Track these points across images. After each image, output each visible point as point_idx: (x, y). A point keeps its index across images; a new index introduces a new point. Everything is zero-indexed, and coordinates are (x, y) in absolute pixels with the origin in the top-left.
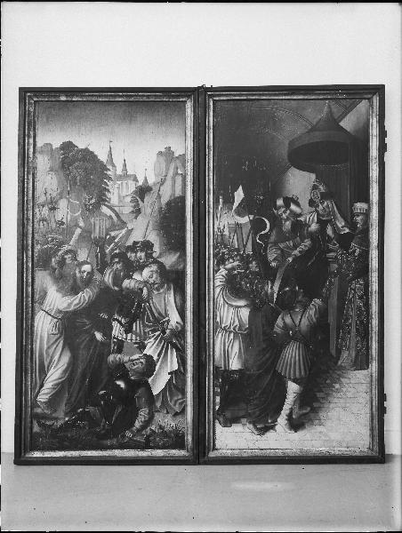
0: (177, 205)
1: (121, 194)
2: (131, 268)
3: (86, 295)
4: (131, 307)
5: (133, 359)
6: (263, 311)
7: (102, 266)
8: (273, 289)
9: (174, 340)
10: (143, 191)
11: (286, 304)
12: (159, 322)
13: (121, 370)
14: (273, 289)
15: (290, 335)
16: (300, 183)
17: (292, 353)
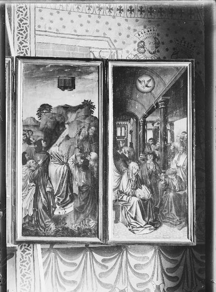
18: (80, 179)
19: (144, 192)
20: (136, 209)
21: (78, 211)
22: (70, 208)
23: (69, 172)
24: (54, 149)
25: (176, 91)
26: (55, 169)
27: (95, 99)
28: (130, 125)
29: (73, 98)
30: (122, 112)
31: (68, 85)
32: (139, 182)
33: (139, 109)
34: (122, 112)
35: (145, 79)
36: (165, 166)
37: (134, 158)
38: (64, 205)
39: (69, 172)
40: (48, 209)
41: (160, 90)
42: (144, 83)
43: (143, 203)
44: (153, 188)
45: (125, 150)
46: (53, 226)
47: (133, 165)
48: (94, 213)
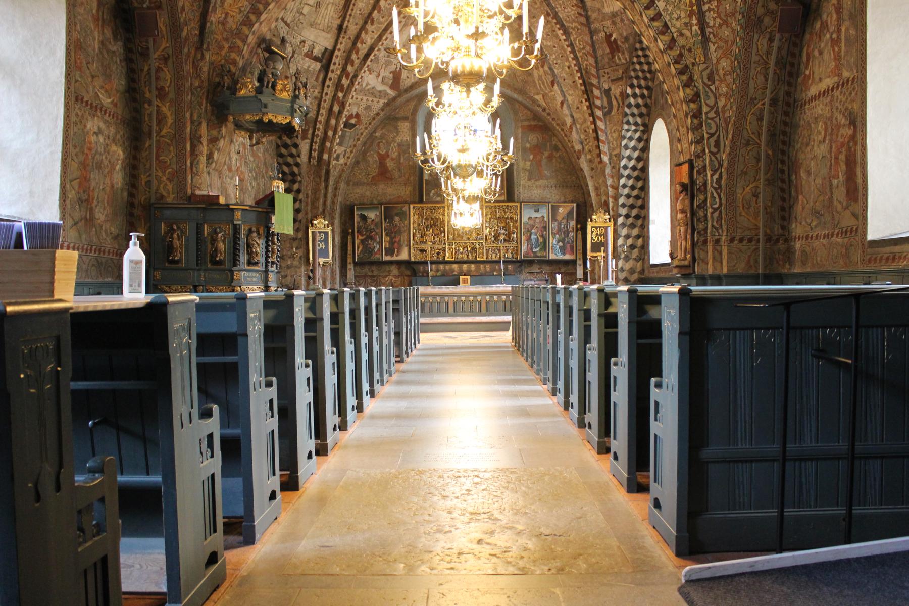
0: (378, 222)
1: (369, 221)
2: (371, 232)
3: (364, 237)
4: (371, 238)
5: (372, 246)
6: (392, 239)
7: (367, 232)
8: (393, 235)
9: (378, 243)
10: (373, 220)
11: (395, 237)
12: (376, 240)
13: (370, 248)
14: (393, 235)
15: (395, 242)
16: (397, 218)
17: (396, 244)
18: (541, 240)
19: (561, 244)
20: (558, 249)
21: (540, 250)
22: (538, 249)
23: (538, 238)
24: (533, 231)
25: (570, 214)
26: (533, 237)
27: (546, 216)
28: (556, 223)
29: (538, 215)
30: (554, 219)
31: (537, 211)
32: (559, 241)
33: (559, 218)
34: (554, 219)
35: (561, 209)
36: (568, 236)
37: (558, 234)
38: (536, 248)
39: (538, 238)
40: (532, 249)
41: (566, 212)
42: (561, 210)
43: (560, 247)
44: (563, 242)
45: (555, 231)
46: (532, 255)
47: (557, 236)
48: (545, 251)
